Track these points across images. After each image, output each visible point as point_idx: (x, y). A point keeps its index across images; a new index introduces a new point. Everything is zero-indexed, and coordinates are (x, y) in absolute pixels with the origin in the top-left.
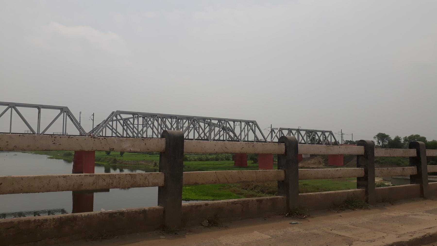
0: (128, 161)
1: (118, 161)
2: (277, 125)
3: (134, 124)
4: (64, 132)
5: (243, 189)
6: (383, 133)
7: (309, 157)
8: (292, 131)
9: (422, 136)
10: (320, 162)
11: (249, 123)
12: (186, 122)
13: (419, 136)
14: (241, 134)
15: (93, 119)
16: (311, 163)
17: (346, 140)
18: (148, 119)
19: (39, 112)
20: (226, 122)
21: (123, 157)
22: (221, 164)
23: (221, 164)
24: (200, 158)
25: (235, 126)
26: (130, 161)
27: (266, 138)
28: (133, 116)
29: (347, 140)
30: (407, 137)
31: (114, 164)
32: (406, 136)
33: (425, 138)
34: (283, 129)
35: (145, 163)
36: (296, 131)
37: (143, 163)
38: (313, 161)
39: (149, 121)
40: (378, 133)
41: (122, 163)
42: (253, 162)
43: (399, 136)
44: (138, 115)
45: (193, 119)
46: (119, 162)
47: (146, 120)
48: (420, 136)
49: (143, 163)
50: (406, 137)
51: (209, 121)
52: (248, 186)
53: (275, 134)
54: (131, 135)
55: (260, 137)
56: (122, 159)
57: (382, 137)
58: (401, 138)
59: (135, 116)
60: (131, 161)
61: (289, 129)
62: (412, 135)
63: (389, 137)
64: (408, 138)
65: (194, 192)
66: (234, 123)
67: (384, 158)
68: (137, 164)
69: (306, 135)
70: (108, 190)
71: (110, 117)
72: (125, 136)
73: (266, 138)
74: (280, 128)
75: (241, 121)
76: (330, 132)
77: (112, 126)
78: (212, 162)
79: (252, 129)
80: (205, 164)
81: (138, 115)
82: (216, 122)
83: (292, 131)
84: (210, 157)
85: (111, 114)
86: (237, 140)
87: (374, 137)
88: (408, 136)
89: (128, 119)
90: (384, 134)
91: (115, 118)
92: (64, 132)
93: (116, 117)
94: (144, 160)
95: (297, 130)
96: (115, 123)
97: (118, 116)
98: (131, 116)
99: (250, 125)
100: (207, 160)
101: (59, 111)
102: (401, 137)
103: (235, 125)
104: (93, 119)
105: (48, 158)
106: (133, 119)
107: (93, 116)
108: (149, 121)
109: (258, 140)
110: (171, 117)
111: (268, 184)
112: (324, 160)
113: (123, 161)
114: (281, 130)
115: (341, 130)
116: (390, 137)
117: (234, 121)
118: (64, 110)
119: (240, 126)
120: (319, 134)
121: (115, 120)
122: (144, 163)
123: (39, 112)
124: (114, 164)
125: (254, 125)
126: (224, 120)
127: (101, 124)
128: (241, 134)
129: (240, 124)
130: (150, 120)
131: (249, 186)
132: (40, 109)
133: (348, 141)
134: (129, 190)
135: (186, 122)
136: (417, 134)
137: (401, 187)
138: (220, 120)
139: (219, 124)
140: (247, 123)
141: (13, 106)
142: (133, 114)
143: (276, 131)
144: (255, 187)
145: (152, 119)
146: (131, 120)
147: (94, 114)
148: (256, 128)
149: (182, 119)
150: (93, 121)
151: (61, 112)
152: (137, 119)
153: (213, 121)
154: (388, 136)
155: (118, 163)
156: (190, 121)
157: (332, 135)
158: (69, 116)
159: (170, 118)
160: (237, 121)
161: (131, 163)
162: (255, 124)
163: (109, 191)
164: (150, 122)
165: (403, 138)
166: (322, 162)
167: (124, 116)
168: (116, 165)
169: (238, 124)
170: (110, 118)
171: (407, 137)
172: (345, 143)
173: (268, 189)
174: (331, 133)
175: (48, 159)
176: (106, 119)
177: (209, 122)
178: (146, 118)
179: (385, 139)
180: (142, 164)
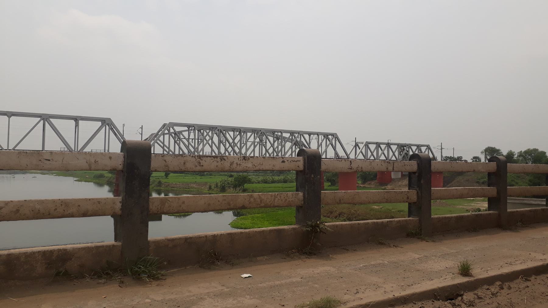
0: (175, 184)
1: (163, 184)
2: (363, 139)
3: (190, 138)
4: (107, 149)
5: (325, 217)
7: (400, 177)
9: (541, 150)
11: (328, 136)
12: (251, 135)
13: (537, 150)
15: (141, 133)
16: (403, 185)
17: (445, 156)
18: (205, 134)
19: (77, 125)
20: (300, 135)
22: (291, 187)
23: (291, 187)
24: (264, 180)
25: (311, 140)
27: (349, 154)
28: (188, 129)
29: (446, 156)
31: (159, 188)
32: (520, 151)
33: (545, 153)
34: (370, 144)
35: (197, 187)
36: (385, 145)
37: (194, 186)
39: (206, 136)
40: (487, 147)
41: (168, 186)
42: (330, 184)
43: (513, 151)
44: (194, 127)
45: (261, 132)
46: (165, 185)
47: (203, 134)
49: (194, 186)
50: (521, 151)
51: (280, 134)
52: (331, 214)
53: (361, 149)
54: (186, 151)
55: (341, 154)
56: (168, 182)
58: (515, 153)
59: (191, 128)
61: (377, 142)
62: (529, 149)
64: (523, 152)
65: (267, 221)
66: (310, 136)
68: (187, 187)
69: (417, 150)
70: (160, 219)
71: (161, 131)
72: (177, 152)
73: (349, 154)
74: (366, 142)
75: (318, 134)
76: (427, 146)
77: (163, 143)
78: (280, 185)
79: (331, 144)
81: (195, 128)
82: (287, 135)
85: (162, 127)
87: (481, 152)
88: (523, 151)
89: (181, 132)
90: (494, 148)
91: (166, 132)
92: (107, 149)
93: (169, 131)
94: (196, 182)
96: (167, 137)
97: (171, 129)
98: (186, 128)
99: (329, 138)
101: (99, 124)
103: (311, 138)
104: (142, 133)
105: (75, 181)
106: (189, 133)
107: (142, 129)
108: (206, 136)
109: (338, 157)
110: (234, 129)
111: (356, 211)
113: (169, 184)
114: (367, 145)
116: (501, 152)
117: (310, 134)
118: (106, 123)
119: (317, 140)
120: (414, 148)
121: (167, 134)
123: (77, 125)
124: (159, 188)
125: (334, 139)
126: (299, 133)
127: (148, 139)
129: (317, 138)
130: (208, 134)
131: (331, 213)
132: (78, 121)
133: (448, 157)
134: (185, 218)
135: (251, 135)
138: (292, 133)
139: (291, 138)
140: (326, 136)
141: (45, 118)
142: (189, 126)
143: (361, 146)
144: (340, 215)
145: (210, 134)
146: (186, 134)
147: (142, 127)
148: (337, 142)
149: (245, 132)
150: (142, 135)
151: (102, 124)
152: (193, 132)
153: (285, 135)
155: (163, 186)
156: (257, 135)
157: (430, 151)
158: (112, 129)
159: (233, 130)
160: (314, 133)
162: (335, 137)
163: (160, 219)
164: (208, 138)
165: (518, 153)
167: (178, 129)
168: (161, 188)
170: (161, 132)
173: (356, 217)
174: (428, 147)
175: (75, 181)
176: (156, 132)
177: (280, 135)
178: (202, 131)
179: (495, 155)
180: (193, 187)
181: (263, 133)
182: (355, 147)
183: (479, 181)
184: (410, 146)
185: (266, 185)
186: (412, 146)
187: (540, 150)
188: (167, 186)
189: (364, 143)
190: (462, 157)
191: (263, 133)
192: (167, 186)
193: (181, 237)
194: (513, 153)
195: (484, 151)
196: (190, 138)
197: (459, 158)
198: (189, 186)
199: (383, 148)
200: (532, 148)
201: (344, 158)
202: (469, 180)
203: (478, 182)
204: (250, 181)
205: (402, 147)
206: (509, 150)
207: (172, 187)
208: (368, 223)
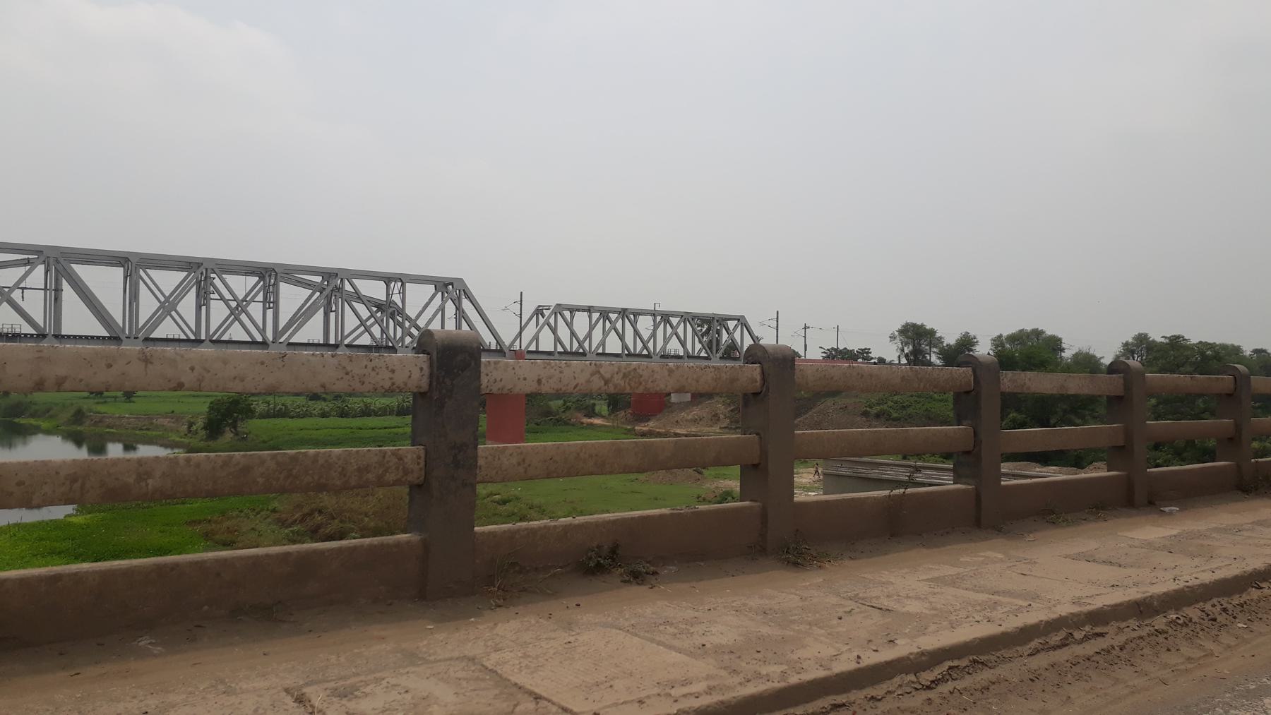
0: (119, 417)
1: (87, 417)
6: (919, 323)
7: (690, 400)
9: (1049, 334)
10: (716, 415)
11: (446, 285)
13: (1042, 332)
14: (589, 335)
16: (686, 421)
17: (829, 348)
21: (134, 402)
22: (385, 428)
23: (385, 428)
26: (128, 418)
30: (1044, 336)
32: (998, 334)
34: (578, 310)
36: (616, 315)
37: (165, 422)
38: (696, 412)
40: (903, 323)
41: (100, 422)
43: (972, 334)
46: (92, 421)
48: (1047, 333)
49: (165, 422)
50: (1000, 336)
56: (102, 411)
58: (975, 340)
60: (131, 418)
62: (1021, 331)
63: (938, 335)
64: (1006, 339)
68: (144, 426)
74: (558, 305)
76: (739, 320)
80: (327, 428)
82: (318, 279)
84: (379, 402)
86: (581, 351)
87: (890, 337)
88: (1005, 334)
90: (922, 325)
94: (173, 412)
95: (620, 312)
100: (367, 412)
102: (977, 337)
109: (501, 347)
112: (732, 411)
113: (104, 416)
116: (941, 338)
117: (388, 279)
122: (169, 424)
128: (589, 335)
137: (844, 500)
143: (547, 313)
155: (88, 423)
157: (745, 328)
161: (129, 424)
166: (722, 416)
169: (396, 291)
171: (1044, 336)
172: (828, 357)
174: (742, 322)
180: (163, 426)
182: (668, 322)
183: (868, 409)
184: (723, 320)
186: (610, 312)
187: (1049, 332)
188: (96, 424)
189: (552, 308)
190: (869, 349)
192: (96, 424)
193: (16, 575)
194: (972, 339)
195: (897, 333)
197: (865, 353)
198: (152, 424)
199: (731, 327)
200: (1029, 328)
201: (332, 341)
202: (846, 407)
203: (865, 414)
204: (249, 413)
205: (709, 325)
206: (964, 331)
207: (108, 427)
208: (175, 566)
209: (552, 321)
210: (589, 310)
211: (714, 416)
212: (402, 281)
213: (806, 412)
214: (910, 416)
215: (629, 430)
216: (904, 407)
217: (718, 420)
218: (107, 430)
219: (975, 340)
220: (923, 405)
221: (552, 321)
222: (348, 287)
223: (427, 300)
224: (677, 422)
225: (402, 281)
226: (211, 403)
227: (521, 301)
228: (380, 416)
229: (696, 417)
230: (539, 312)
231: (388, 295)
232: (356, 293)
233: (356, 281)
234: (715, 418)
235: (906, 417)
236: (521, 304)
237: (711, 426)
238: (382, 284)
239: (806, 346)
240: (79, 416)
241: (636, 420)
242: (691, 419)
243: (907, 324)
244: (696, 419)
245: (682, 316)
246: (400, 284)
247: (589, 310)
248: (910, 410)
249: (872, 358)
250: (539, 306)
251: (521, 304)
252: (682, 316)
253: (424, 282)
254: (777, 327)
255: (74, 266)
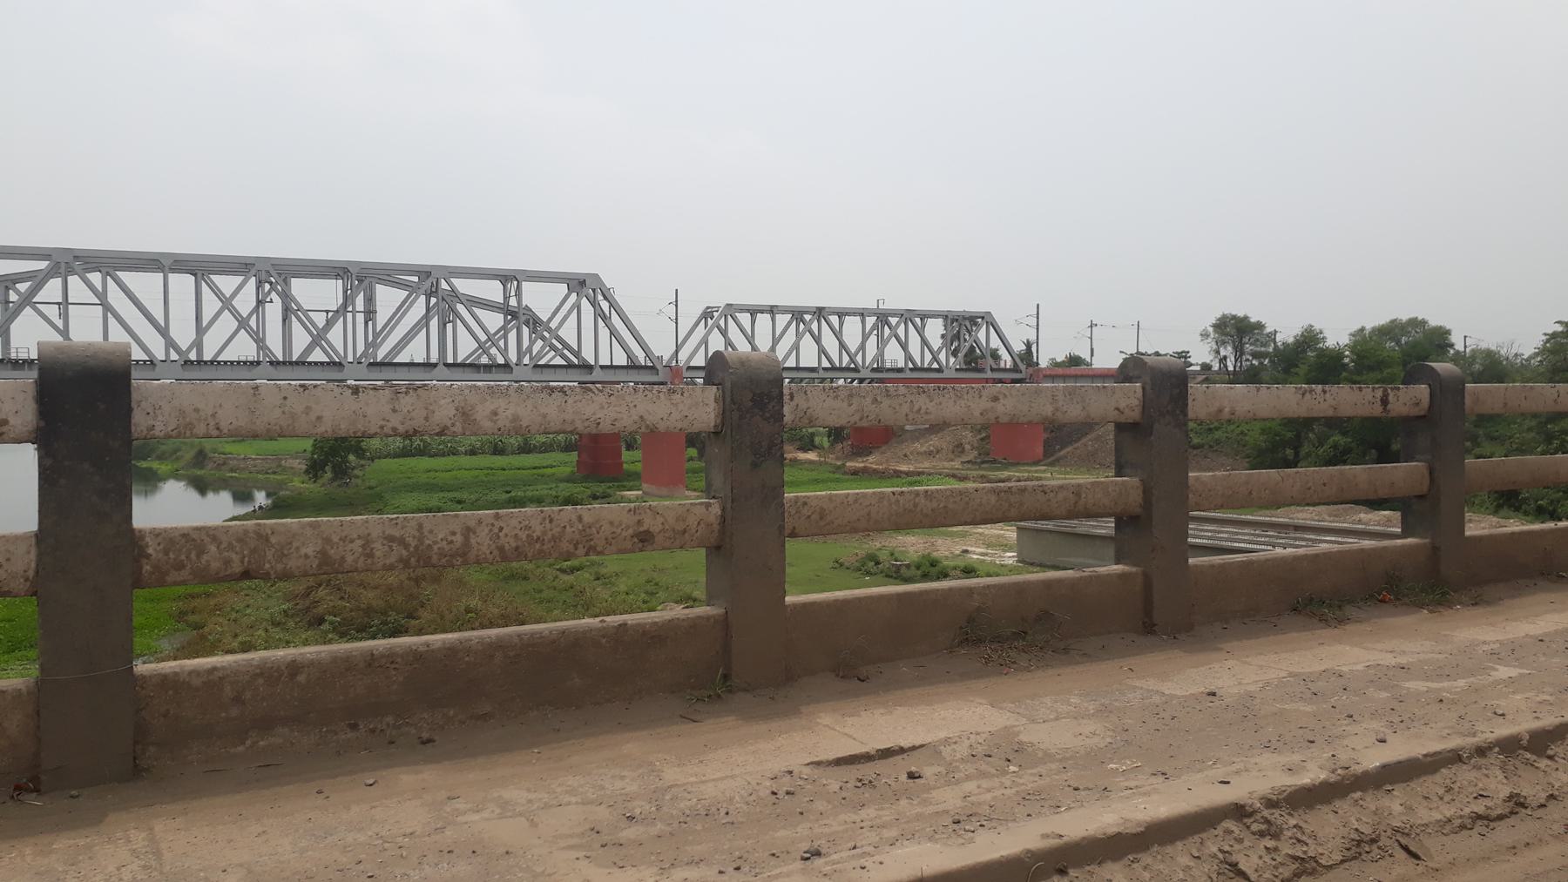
0: (244, 459)
6: (1241, 314)
8: (890, 318)
13: (1423, 323)
14: (862, 347)
32: (1360, 327)
33: (1448, 332)
38: (934, 441)
41: (224, 464)
43: (1317, 327)
48: (1430, 323)
50: (1363, 329)
57: (1235, 330)
58: (1322, 336)
61: (772, 307)
67: (1212, 426)
74: (728, 305)
83: (890, 318)
86: (853, 366)
87: (1201, 335)
88: (1369, 326)
102: (1324, 331)
115: (1038, 305)
117: (506, 278)
120: (935, 329)
128: (862, 347)
136: (1412, 315)
154: (1260, 326)
155: (211, 465)
165: (1351, 335)
166: (968, 447)
180: (292, 468)
181: (63, 265)
185: (499, 461)
187: (1434, 321)
189: (721, 309)
190: (1188, 352)
191: (63, 265)
192: (219, 466)
195: (1211, 329)
196: (70, 301)
198: (280, 466)
205: (961, 325)
206: (1306, 324)
207: (232, 470)
209: (722, 323)
210: (772, 310)
211: (957, 446)
212: (517, 280)
213: (1079, 439)
214: (1218, 442)
215: (839, 468)
216: (1210, 429)
217: (963, 451)
218: (230, 474)
219: (1322, 336)
220: (1238, 427)
221: (722, 323)
222: (444, 285)
223: (558, 304)
224: (905, 455)
225: (517, 280)
226: (315, 441)
227: (677, 301)
228: (541, 452)
229: (932, 448)
230: (707, 314)
231: (505, 298)
232: (453, 291)
233: (454, 281)
234: (959, 449)
235: (1212, 444)
236: (676, 306)
237: (952, 460)
238: (497, 285)
239: (1092, 350)
240: (201, 458)
241: (854, 454)
242: (925, 452)
243: (1224, 317)
244: (932, 451)
245: (902, 315)
246: (516, 283)
247: (772, 311)
248: (1217, 434)
249: (1191, 365)
250: (708, 308)
251: (676, 306)
252: (902, 315)
253: (537, 279)
254: (1038, 325)
255: (117, 273)
